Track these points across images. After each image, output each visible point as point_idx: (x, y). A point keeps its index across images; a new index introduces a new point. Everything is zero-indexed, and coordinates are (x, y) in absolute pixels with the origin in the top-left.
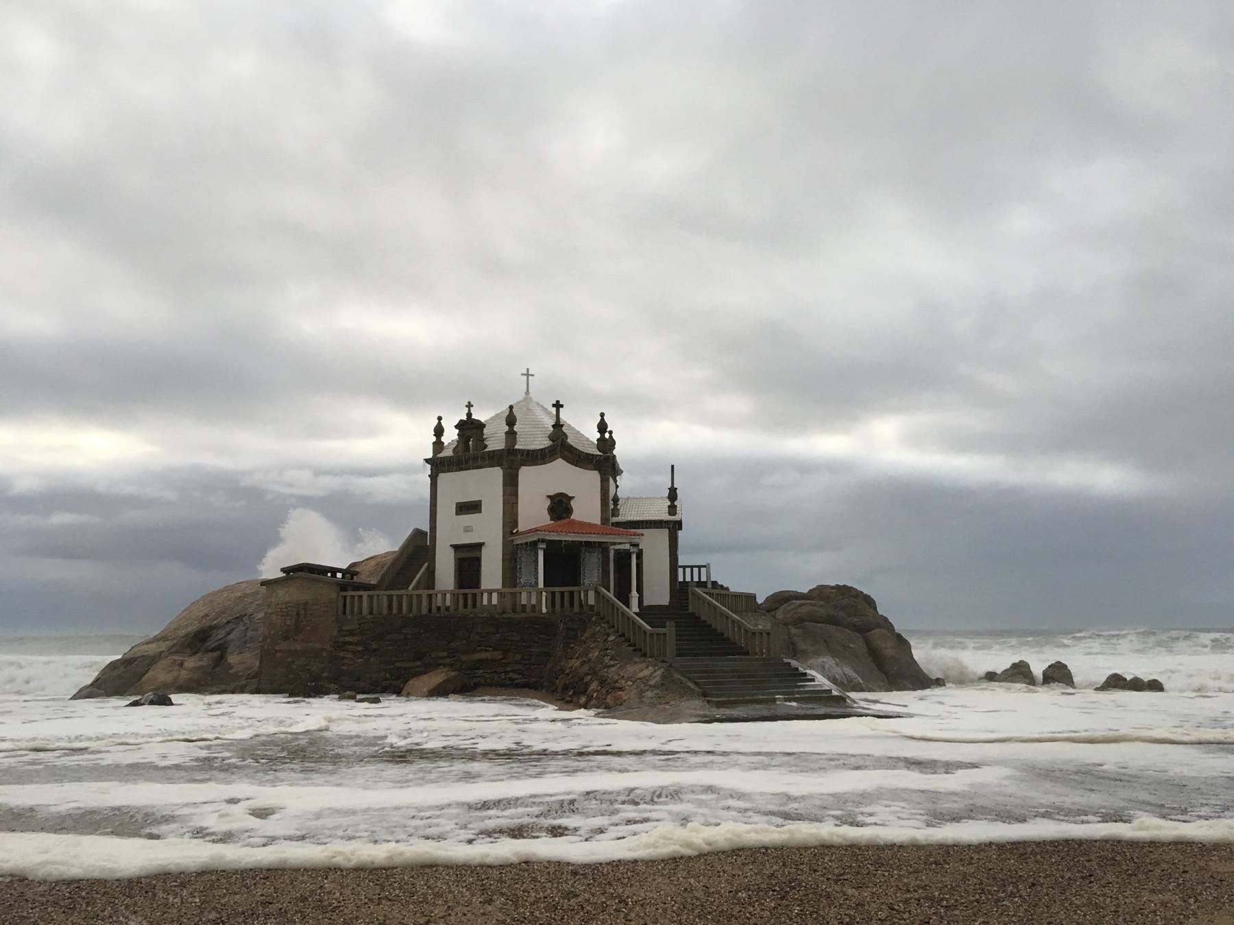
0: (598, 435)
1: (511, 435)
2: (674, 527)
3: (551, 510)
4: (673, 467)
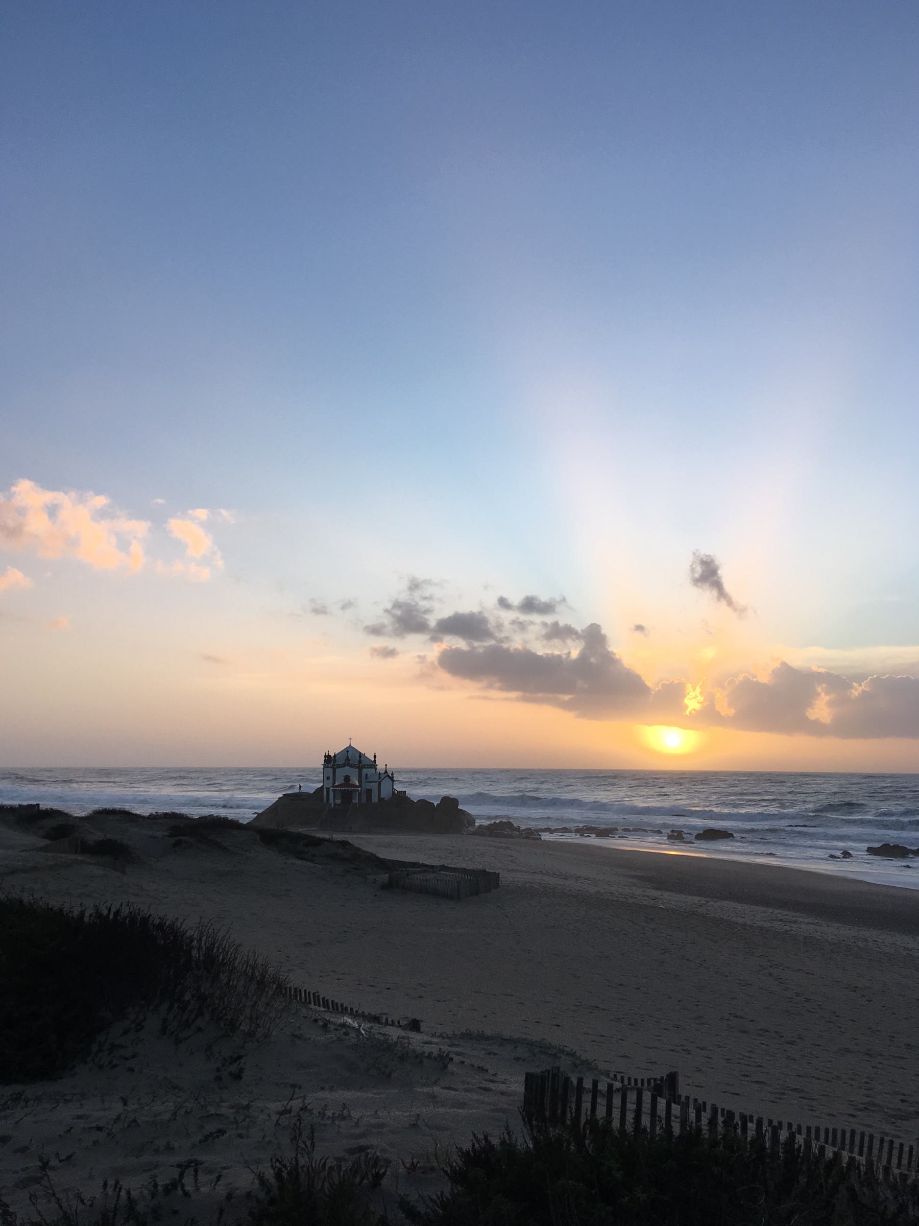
0: (359, 759)
1: (335, 761)
2: (380, 783)
3: (344, 780)
4: (386, 765)
